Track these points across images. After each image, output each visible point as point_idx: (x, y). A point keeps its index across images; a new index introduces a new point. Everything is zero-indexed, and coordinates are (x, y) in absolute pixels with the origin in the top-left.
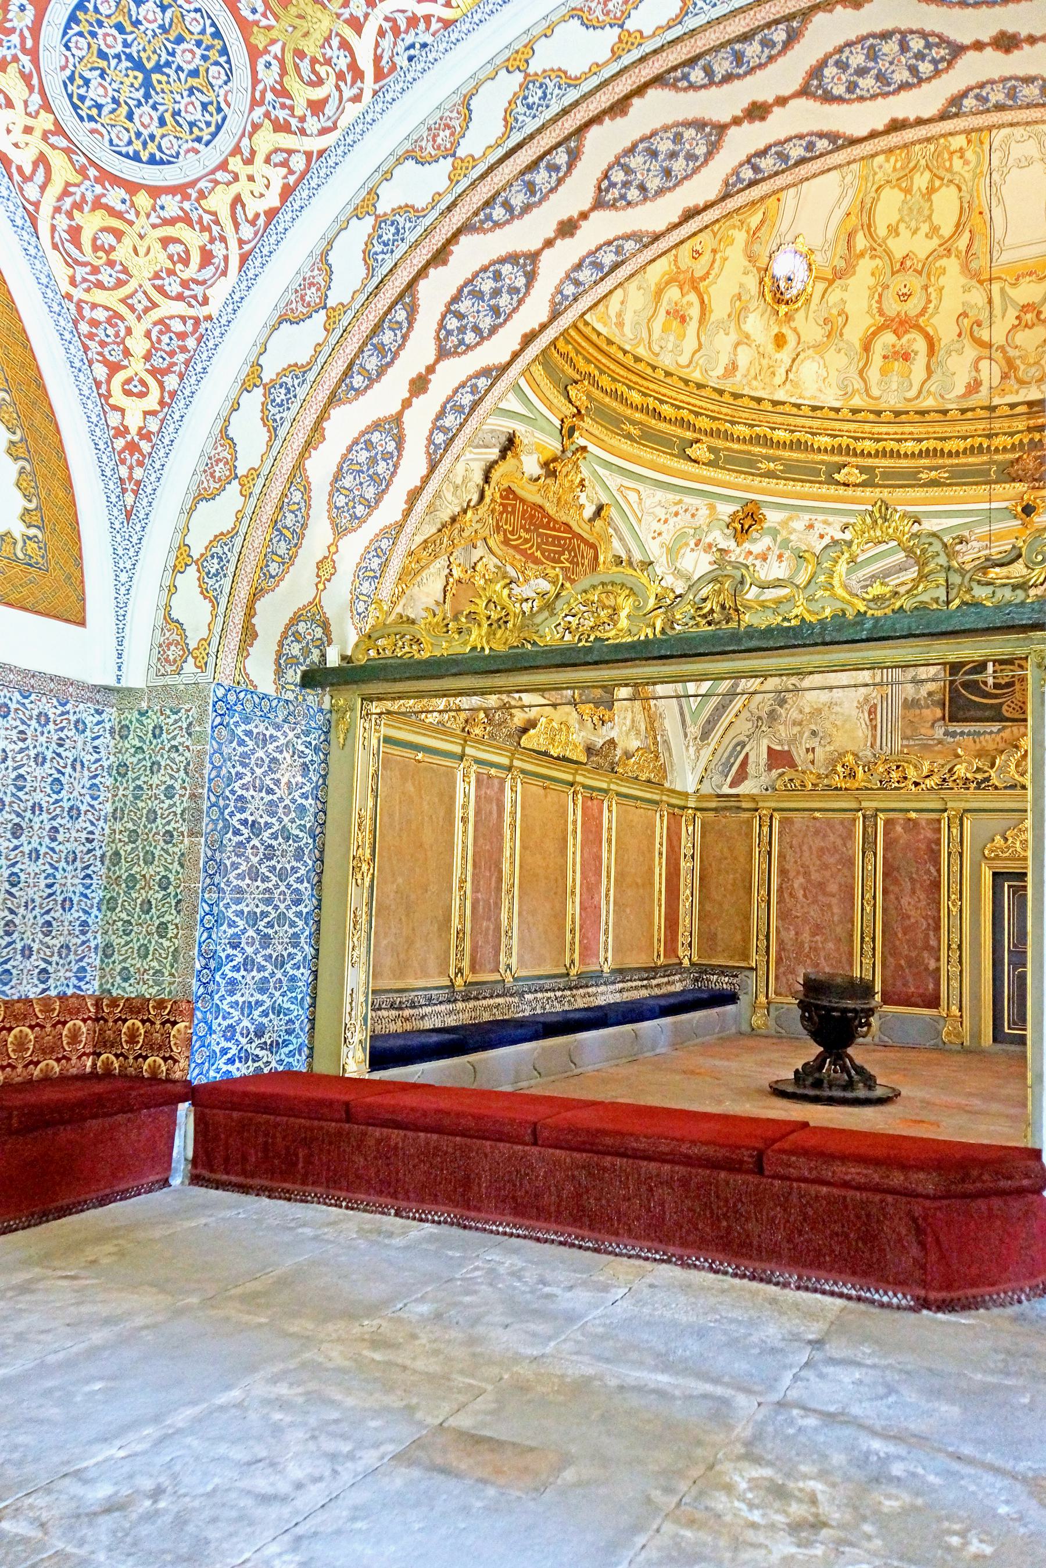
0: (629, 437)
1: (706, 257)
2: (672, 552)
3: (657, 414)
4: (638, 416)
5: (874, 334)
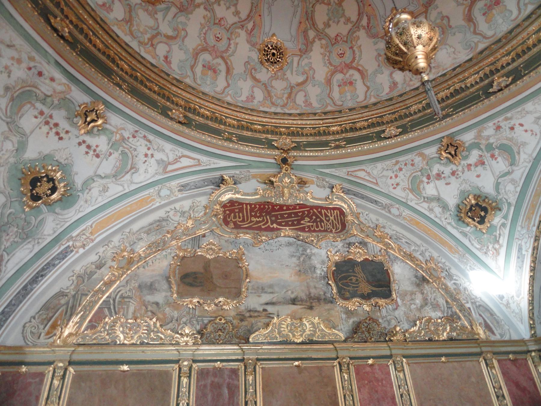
0: (337, 147)
1: (349, 53)
2: (415, 188)
3: (352, 130)
4: (338, 137)
5: (470, 10)
